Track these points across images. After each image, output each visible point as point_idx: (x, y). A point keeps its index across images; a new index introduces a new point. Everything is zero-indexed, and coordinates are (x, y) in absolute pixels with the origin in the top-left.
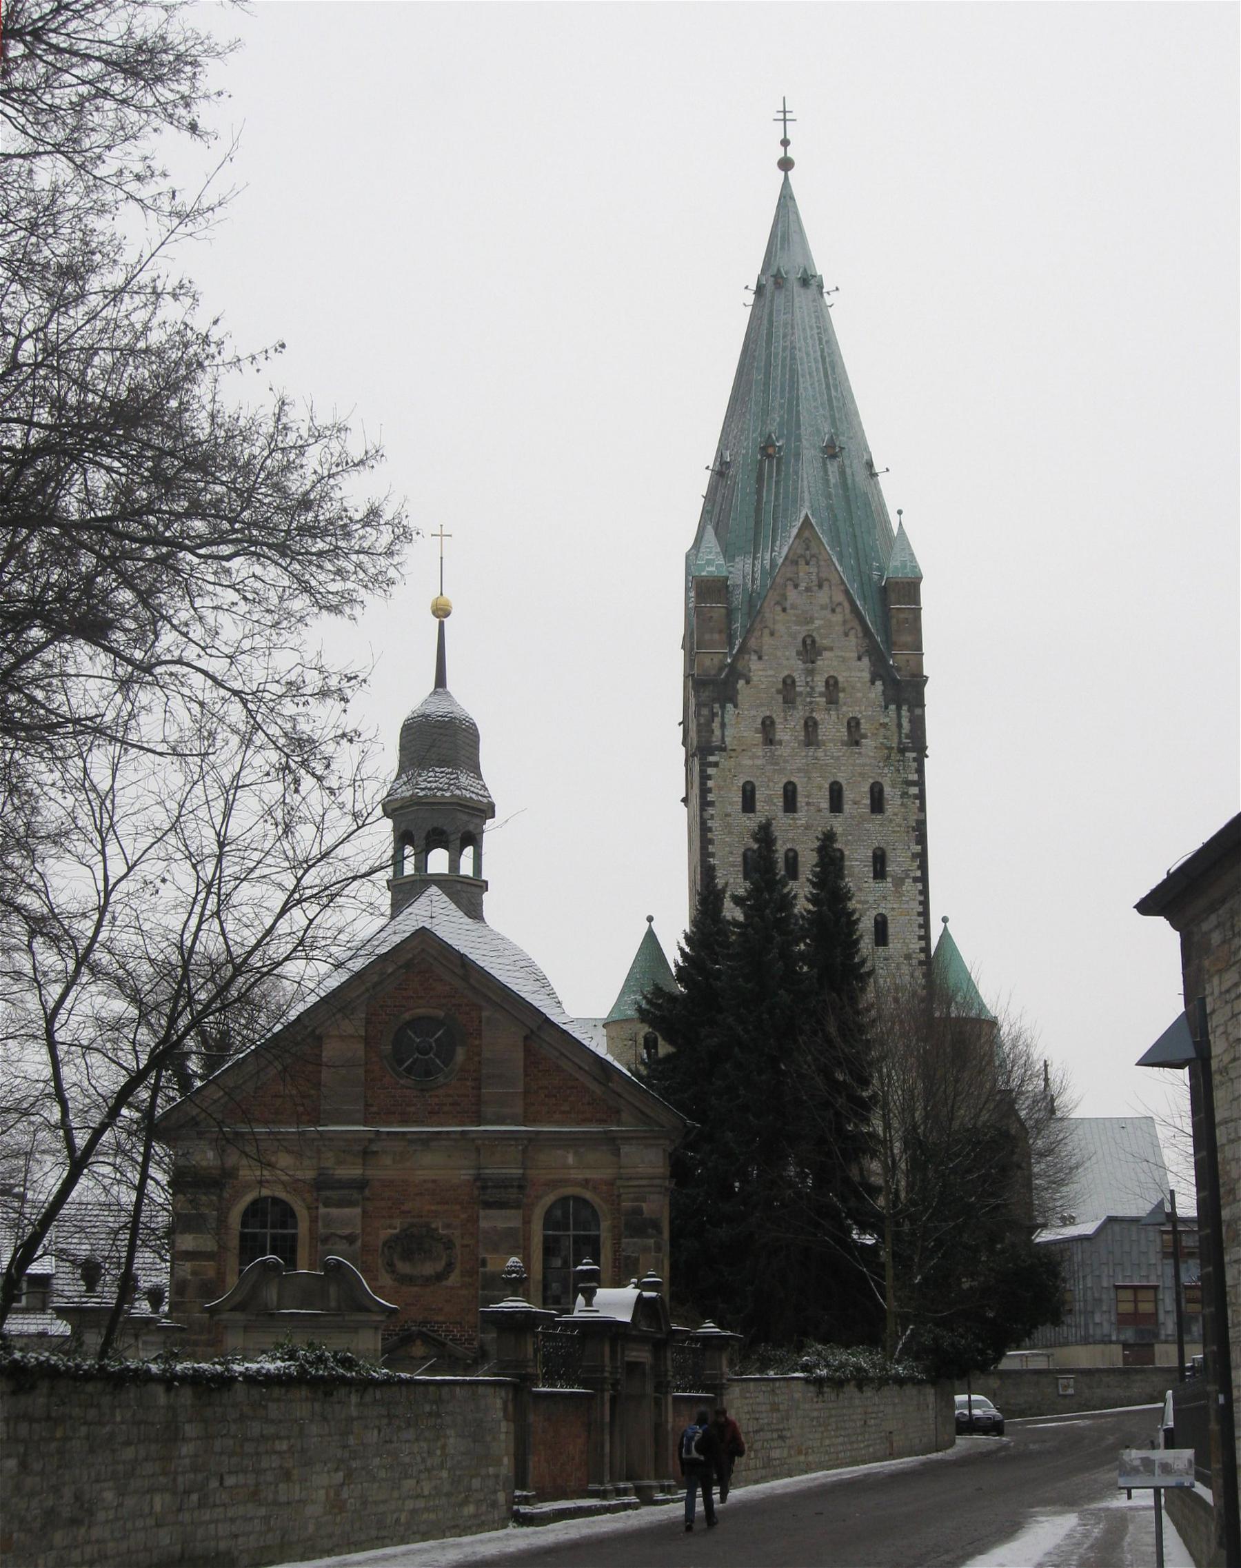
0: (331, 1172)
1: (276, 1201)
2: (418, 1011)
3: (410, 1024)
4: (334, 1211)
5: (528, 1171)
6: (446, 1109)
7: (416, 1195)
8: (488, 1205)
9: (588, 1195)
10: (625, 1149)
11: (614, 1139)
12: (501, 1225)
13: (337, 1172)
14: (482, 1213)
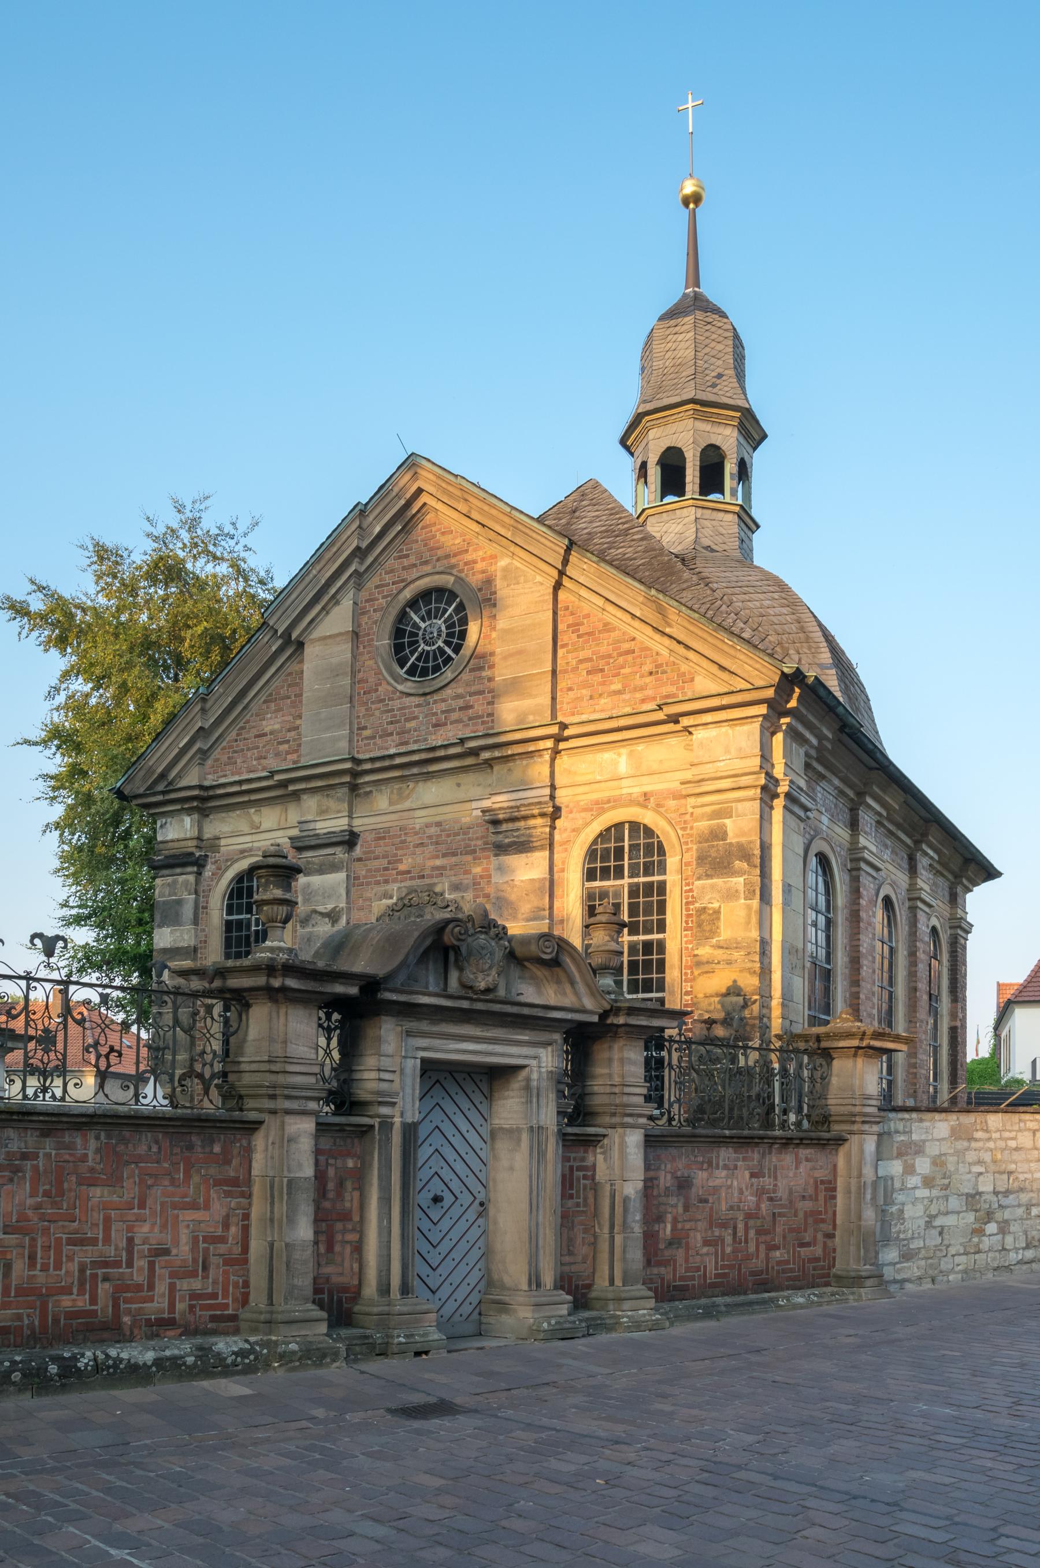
0: (312, 826)
2: (418, 583)
3: (413, 604)
6: (454, 716)
9: (648, 818)
13: (319, 825)
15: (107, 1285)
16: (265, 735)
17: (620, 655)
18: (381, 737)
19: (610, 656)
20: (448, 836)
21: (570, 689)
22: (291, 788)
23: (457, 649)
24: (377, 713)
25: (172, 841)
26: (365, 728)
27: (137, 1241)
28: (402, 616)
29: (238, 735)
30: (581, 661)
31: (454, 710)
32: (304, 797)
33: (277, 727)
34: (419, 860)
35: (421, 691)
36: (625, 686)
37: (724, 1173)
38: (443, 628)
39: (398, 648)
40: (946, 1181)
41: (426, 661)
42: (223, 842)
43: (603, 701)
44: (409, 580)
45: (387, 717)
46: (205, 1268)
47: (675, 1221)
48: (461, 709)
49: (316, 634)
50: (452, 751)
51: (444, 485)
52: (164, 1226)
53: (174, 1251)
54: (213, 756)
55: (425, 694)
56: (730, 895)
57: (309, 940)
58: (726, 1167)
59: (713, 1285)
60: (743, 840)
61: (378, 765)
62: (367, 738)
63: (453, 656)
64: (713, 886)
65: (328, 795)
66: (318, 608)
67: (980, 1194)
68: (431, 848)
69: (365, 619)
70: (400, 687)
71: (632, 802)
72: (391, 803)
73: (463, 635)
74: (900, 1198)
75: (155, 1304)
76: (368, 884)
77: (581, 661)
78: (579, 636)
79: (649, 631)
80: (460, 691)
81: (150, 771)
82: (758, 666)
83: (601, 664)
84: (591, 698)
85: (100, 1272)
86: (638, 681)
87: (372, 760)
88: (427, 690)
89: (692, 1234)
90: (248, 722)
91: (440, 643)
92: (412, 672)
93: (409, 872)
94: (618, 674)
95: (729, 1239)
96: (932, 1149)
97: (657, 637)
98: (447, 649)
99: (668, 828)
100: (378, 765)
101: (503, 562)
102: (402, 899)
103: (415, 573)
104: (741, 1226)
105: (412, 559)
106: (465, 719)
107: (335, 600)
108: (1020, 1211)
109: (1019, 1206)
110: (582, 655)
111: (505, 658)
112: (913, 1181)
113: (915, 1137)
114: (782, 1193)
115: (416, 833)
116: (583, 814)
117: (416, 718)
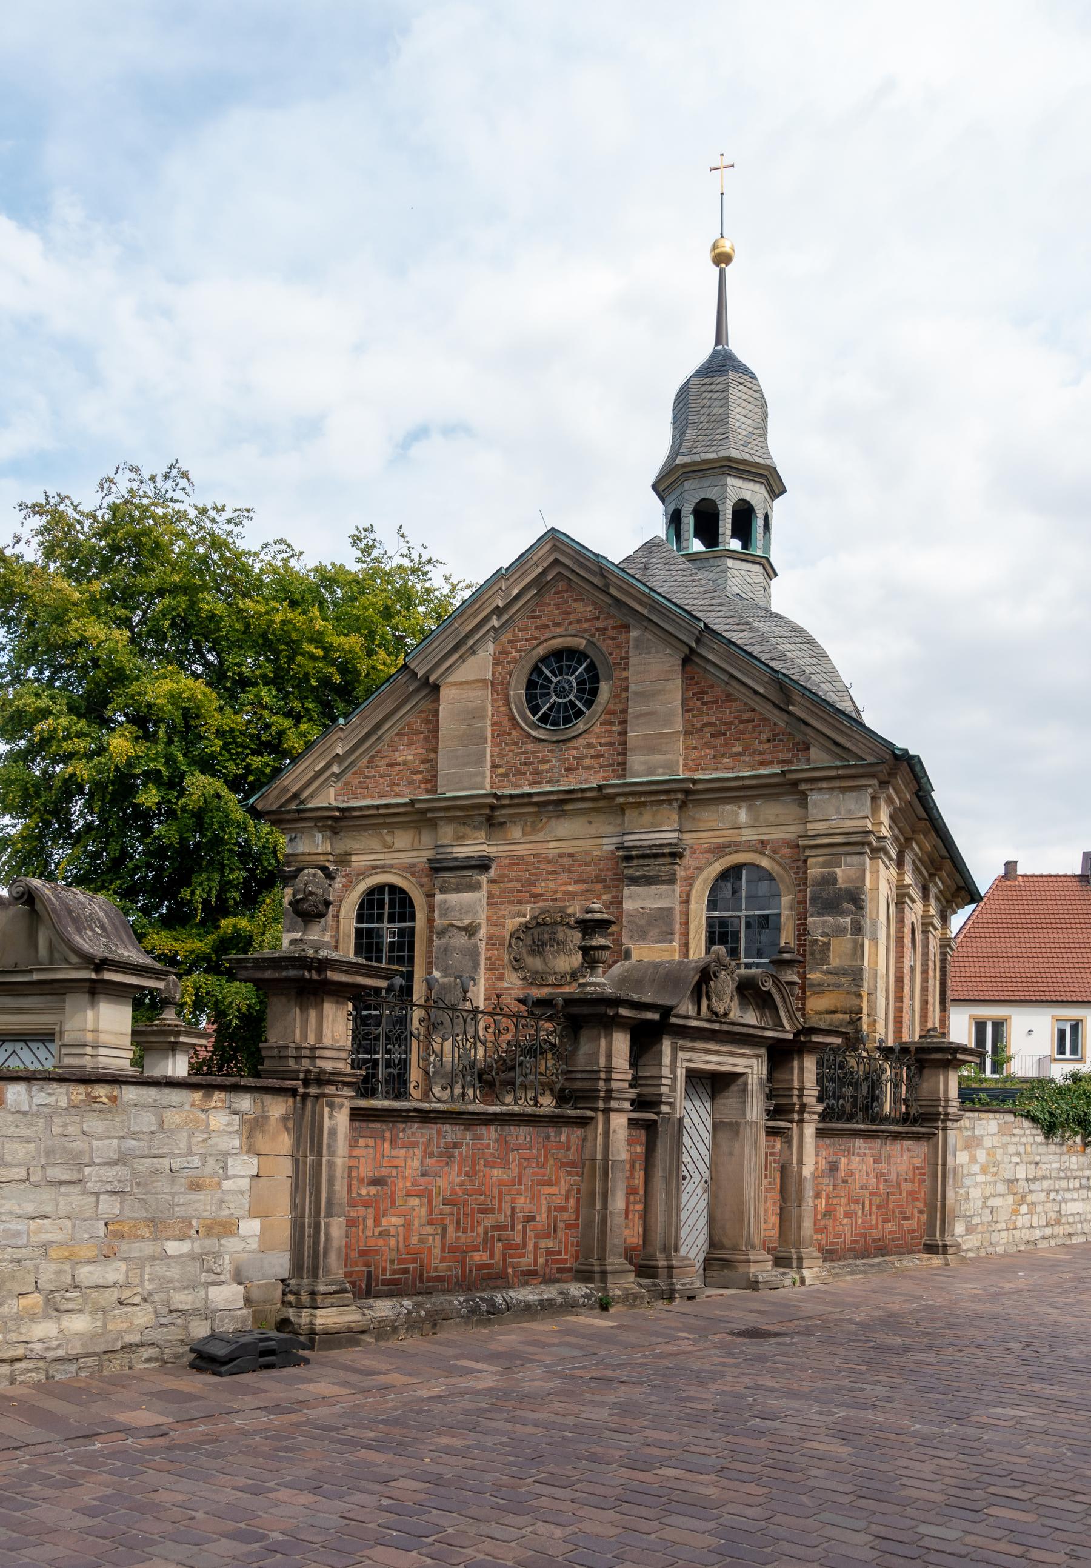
0: (449, 850)
1: (394, 889)
3: (544, 660)
4: (453, 898)
5: (686, 836)
7: (550, 873)
8: (634, 881)
10: (813, 798)
11: (795, 783)
12: (651, 904)
14: (626, 891)
15: (500, 1244)
16: (397, 764)
17: (741, 722)
18: (514, 775)
19: (732, 723)
20: (580, 866)
21: (695, 748)
22: (429, 815)
23: (589, 704)
24: (511, 754)
25: (303, 854)
26: (499, 766)
27: (517, 1210)
28: (536, 669)
29: (369, 762)
30: (705, 725)
31: (585, 758)
32: (441, 823)
33: (410, 758)
34: (551, 884)
35: (555, 739)
36: (745, 750)
37: (858, 1159)
38: (574, 684)
39: (530, 698)
40: (995, 1169)
41: (559, 711)
42: (354, 858)
43: (725, 761)
44: (542, 638)
45: (521, 759)
46: (555, 1231)
47: (828, 1196)
48: (592, 757)
49: (451, 679)
50: (588, 795)
51: (582, 560)
52: (532, 1199)
53: (538, 1218)
54: (343, 779)
55: (558, 742)
56: (840, 931)
57: (445, 950)
58: (859, 1155)
59: (850, 1250)
60: (851, 886)
61: (516, 801)
62: (501, 775)
63: (584, 709)
64: (824, 923)
65: (464, 824)
66: (456, 656)
67: (1017, 1180)
68: (564, 876)
69: (499, 669)
70: (533, 733)
71: (749, 848)
72: (524, 834)
73: (594, 692)
74: (967, 1182)
75: (526, 1259)
76: (502, 903)
77: (705, 725)
78: (703, 703)
79: (770, 707)
80: (592, 741)
81: (285, 789)
82: (870, 745)
83: (723, 729)
84: (714, 757)
85: (496, 1234)
86: (757, 746)
87: (512, 797)
88: (561, 738)
89: (838, 1207)
90: (379, 751)
91: (571, 697)
92: (544, 719)
93: (541, 895)
94: (738, 739)
95: (860, 1213)
96: (987, 1142)
97: (776, 712)
98: (577, 702)
99: (782, 872)
100: (516, 801)
101: (634, 634)
102: (536, 918)
103: (547, 634)
104: (867, 1202)
105: (546, 620)
106: (597, 766)
107: (472, 651)
108: (1043, 1196)
109: (1042, 1191)
110: (705, 720)
111: (638, 717)
112: (976, 1168)
113: (977, 1132)
114: (893, 1176)
115: (549, 862)
116: (706, 856)
117: (549, 761)
